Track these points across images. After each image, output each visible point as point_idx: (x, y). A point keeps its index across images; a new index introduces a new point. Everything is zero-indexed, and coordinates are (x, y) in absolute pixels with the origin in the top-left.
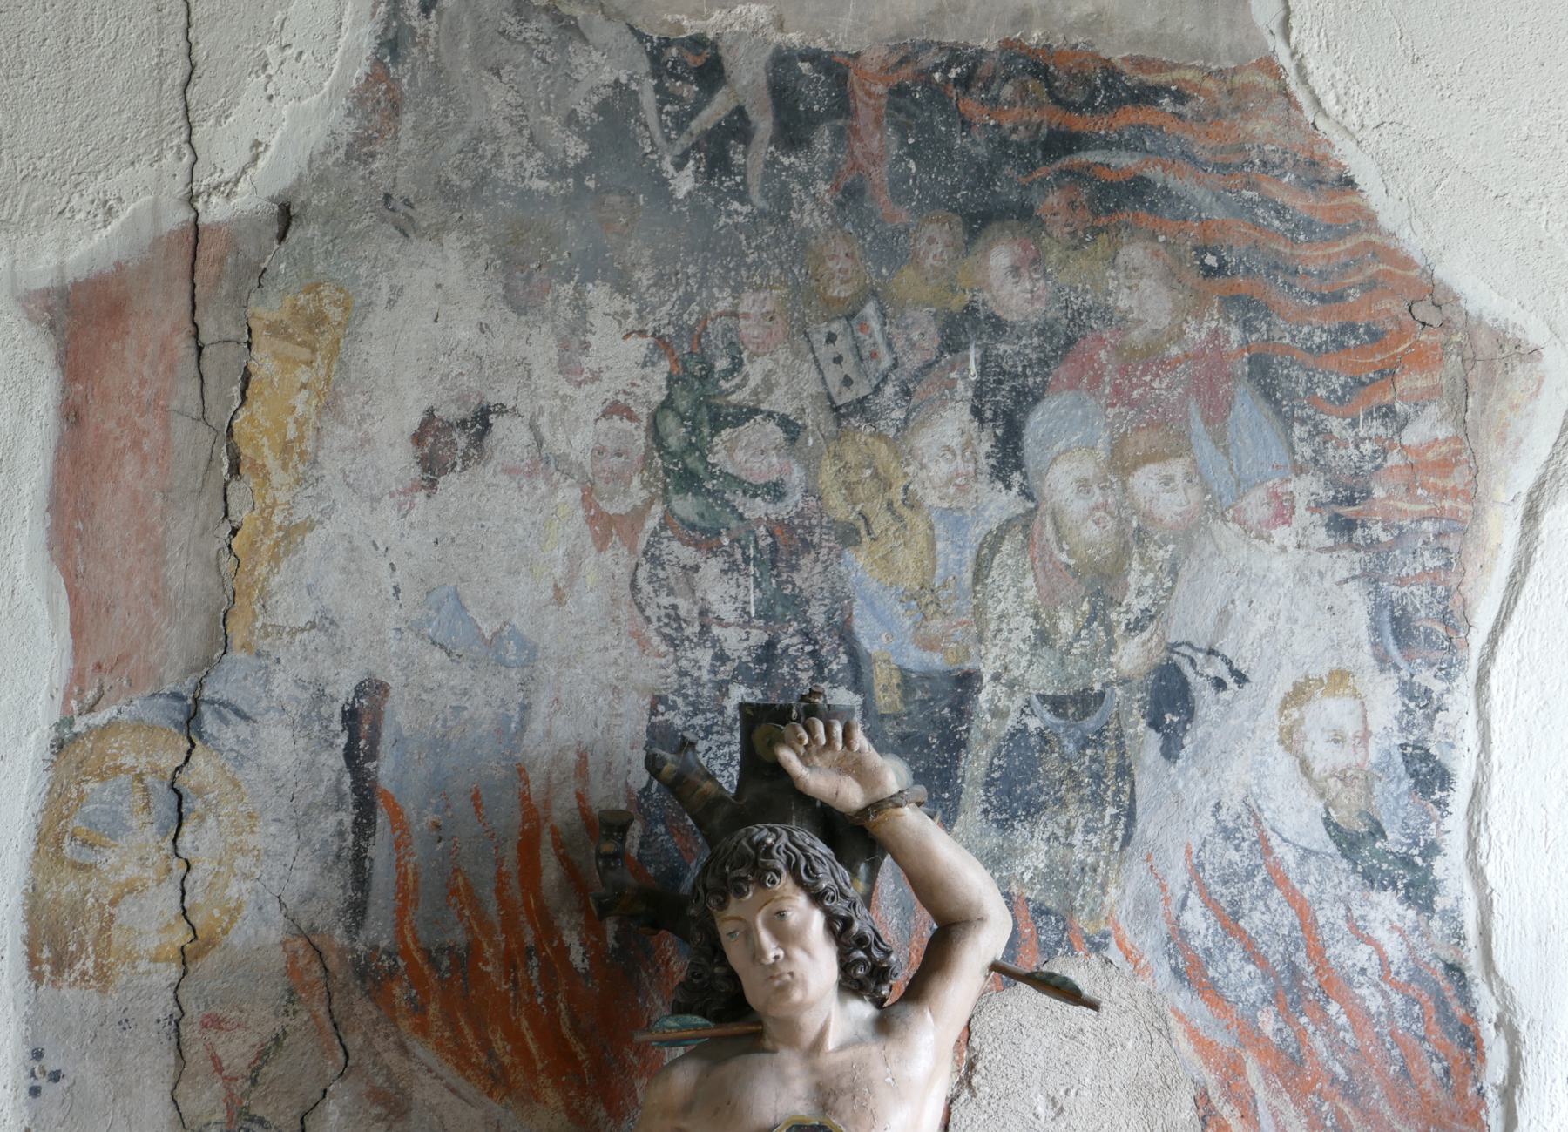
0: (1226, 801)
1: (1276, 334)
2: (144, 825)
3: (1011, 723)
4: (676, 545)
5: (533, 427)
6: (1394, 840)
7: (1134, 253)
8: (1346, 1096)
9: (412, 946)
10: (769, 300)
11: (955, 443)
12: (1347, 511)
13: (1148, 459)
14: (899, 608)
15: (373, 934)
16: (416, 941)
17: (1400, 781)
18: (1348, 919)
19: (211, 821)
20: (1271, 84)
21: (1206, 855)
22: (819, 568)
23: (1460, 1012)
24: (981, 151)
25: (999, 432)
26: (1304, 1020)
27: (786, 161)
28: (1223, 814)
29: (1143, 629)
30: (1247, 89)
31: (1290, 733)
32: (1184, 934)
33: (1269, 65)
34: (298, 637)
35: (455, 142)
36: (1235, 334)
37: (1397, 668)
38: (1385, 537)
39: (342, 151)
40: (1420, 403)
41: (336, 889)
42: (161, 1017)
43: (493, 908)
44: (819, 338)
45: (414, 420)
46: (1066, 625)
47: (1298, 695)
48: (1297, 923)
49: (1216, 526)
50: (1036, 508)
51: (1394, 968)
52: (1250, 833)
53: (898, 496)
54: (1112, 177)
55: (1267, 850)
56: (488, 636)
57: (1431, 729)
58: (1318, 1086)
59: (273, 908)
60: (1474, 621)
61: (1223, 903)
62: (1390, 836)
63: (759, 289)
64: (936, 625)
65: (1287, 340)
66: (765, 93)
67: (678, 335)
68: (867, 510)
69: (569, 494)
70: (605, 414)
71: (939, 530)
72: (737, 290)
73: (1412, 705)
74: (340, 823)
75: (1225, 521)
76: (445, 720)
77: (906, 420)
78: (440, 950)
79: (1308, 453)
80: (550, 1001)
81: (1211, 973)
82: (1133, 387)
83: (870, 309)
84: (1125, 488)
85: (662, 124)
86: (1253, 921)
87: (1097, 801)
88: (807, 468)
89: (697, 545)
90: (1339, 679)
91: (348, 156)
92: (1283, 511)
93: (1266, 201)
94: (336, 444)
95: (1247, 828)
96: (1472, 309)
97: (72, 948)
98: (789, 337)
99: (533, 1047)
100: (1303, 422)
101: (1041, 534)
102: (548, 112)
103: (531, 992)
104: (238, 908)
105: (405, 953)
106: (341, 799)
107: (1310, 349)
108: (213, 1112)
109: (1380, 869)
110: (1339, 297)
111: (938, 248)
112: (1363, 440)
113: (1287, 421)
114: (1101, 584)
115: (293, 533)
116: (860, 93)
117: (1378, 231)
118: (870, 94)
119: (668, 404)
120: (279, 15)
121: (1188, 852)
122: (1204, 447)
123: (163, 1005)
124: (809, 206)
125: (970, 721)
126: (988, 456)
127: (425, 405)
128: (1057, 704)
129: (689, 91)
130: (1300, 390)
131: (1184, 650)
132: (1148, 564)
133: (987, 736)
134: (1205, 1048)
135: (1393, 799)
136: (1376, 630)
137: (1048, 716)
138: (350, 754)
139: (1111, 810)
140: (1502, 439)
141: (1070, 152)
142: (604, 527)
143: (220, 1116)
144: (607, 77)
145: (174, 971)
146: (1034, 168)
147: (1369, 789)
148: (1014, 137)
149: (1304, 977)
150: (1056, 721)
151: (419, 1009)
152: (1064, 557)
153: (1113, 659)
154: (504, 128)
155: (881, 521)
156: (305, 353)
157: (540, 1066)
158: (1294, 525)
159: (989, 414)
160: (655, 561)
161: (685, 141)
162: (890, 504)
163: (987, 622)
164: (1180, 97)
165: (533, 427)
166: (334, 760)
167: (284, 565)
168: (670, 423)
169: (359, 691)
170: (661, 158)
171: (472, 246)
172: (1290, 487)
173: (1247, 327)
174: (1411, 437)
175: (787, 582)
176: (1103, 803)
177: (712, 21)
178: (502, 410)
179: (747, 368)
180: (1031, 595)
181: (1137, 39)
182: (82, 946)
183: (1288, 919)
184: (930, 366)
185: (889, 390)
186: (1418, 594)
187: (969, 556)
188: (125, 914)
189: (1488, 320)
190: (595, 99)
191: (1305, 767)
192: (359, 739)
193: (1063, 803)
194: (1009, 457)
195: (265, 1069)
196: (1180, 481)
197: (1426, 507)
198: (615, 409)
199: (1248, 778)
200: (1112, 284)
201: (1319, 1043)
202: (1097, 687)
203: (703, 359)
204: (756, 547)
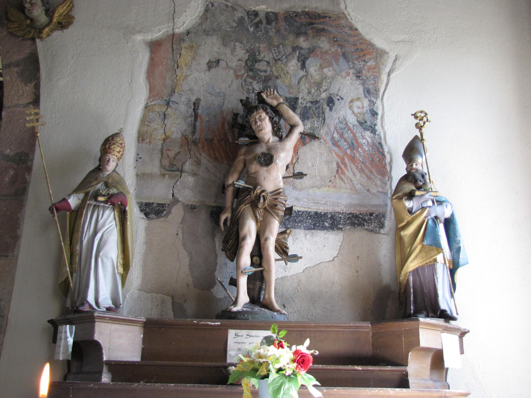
3: (304, 105)
5: (226, 62)
6: (369, 123)
7: (323, 39)
10: (265, 45)
13: (325, 67)
18: (362, 135)
30: (340, 17)
32: (334, 138)
33: (343, 14)
35: (215, 24)
36: (339, 50)
40: (370, 60)
41: (190, 130)
44: (273, 50)
45: (207, 61)
46: (313, 91)
47: (352, 101)
49: (337, 77)
52: (344, 122)
53: (285, 72)
55: (347, 125)
59: (179, 132)
69: (232, 72)
72: (260, 44)
83: (281, 46)
86: (346, 136)
87: (319, 117)
90: (358, 99)
92: (348, 74)
95: (344, 121)
110: (356, 45)
113: (348, 62)
114: (319, 85)
115: (186, 76)
119: (248, 59)
123: (160, 147)
128: (312, 102)
129: (253, 17)
132: (326, 82)
134: (338, 156)
138: (194, 109)
140: (383, 65)
142: (237, 77)
144: (240, 15)
145: (162, 142)
155: (282, 75)
161: (252, 24)
164: (330, 17)
165: (226, 62)
166: (191, 110)
169: (196, 100)
173: (341, 49)
174: (368, 64)
178: (221, 60)
180: (307, 86)
182: (147, 138)
184: (290, 54)
185: (284, 57)
186: (371, 87)
187: (297, 81)
191: (353, 112)
193: (313, 117)
194: (303, 66)
198: (239, 60)
199: (344, 114)
201: (357, 155)
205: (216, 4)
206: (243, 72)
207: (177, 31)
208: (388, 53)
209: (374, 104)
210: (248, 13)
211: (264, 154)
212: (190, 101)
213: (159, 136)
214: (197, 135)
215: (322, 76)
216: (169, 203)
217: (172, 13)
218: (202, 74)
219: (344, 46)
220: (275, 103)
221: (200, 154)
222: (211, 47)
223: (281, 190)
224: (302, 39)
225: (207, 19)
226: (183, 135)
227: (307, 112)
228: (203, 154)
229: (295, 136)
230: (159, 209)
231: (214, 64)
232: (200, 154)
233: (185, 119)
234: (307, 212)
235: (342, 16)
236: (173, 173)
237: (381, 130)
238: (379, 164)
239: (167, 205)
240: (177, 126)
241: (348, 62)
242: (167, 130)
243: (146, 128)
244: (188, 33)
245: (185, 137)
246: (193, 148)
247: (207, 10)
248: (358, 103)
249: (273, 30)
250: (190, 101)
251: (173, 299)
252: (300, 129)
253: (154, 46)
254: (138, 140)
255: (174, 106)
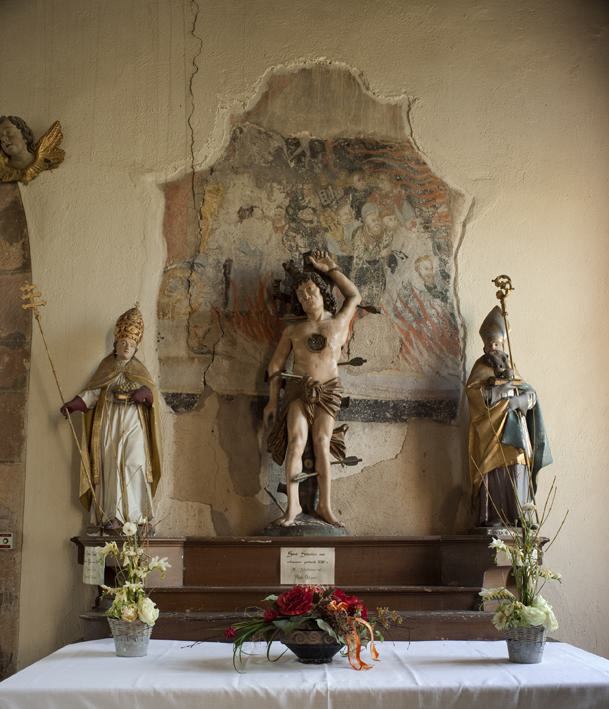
6: (439, 288)
7: (382, 176)
10: (310, 186)
33: (408, 142)
35: (246, 157)
41: (221, 301)
45: (238, 209)
46: (371, 247)
47: (418, 260)
55: (413, 291)
69: (269, 223)
83: (330, 187)
86: (411, 305)
90: (427, 257)
95: (409, 286)
114: (378, 239)
119: (289, 206)
122: (398, 213)
128: (369, 262)
134: (402, 330)
135: (438, 280)
138: (225, 274)
142: (276, 229)
151: (239, 324)
164: (391, 147)
166: (221, 275)
184: (341, 198)
186: (442, 241)
191: (420, 275)
194: (358, 215)
198: (279, 207)
205: (245, 130)
206: (284, 223)
207: (198, 169)
208: (463, 196)
209: (446, 263)
210: (287, 141)
211: (314, 335)
212: (219, 262)
213: (183, 308)
214: (230, 308)
217: (191, 142)
218: (233, 226)
219: (409, 187)
220: (326, 268)
221: (235, 331)
222: (241, 191)
223: (336, 380)
224: (356, 178)
225: (235, 151)
226: (213, 307)
227: (364, 275)
228: (240, 332)
229: (351, 310)
231: (245, 213)
232: (235, 331)
233: (214, 286)
235: (407, 145)
237: (454, 298)
240: (204, 295)
241: (415, 208)
242: (192, 302)
243: (166, 300)
244: (212, 170)
245: (215, 310)
246: (227, 324)
247: (234, 139)
248: (426, 263)
249: (320, 165)
251: (212, 507)
252: (356, 301)
253: (170, 189)
254: (158, 315)
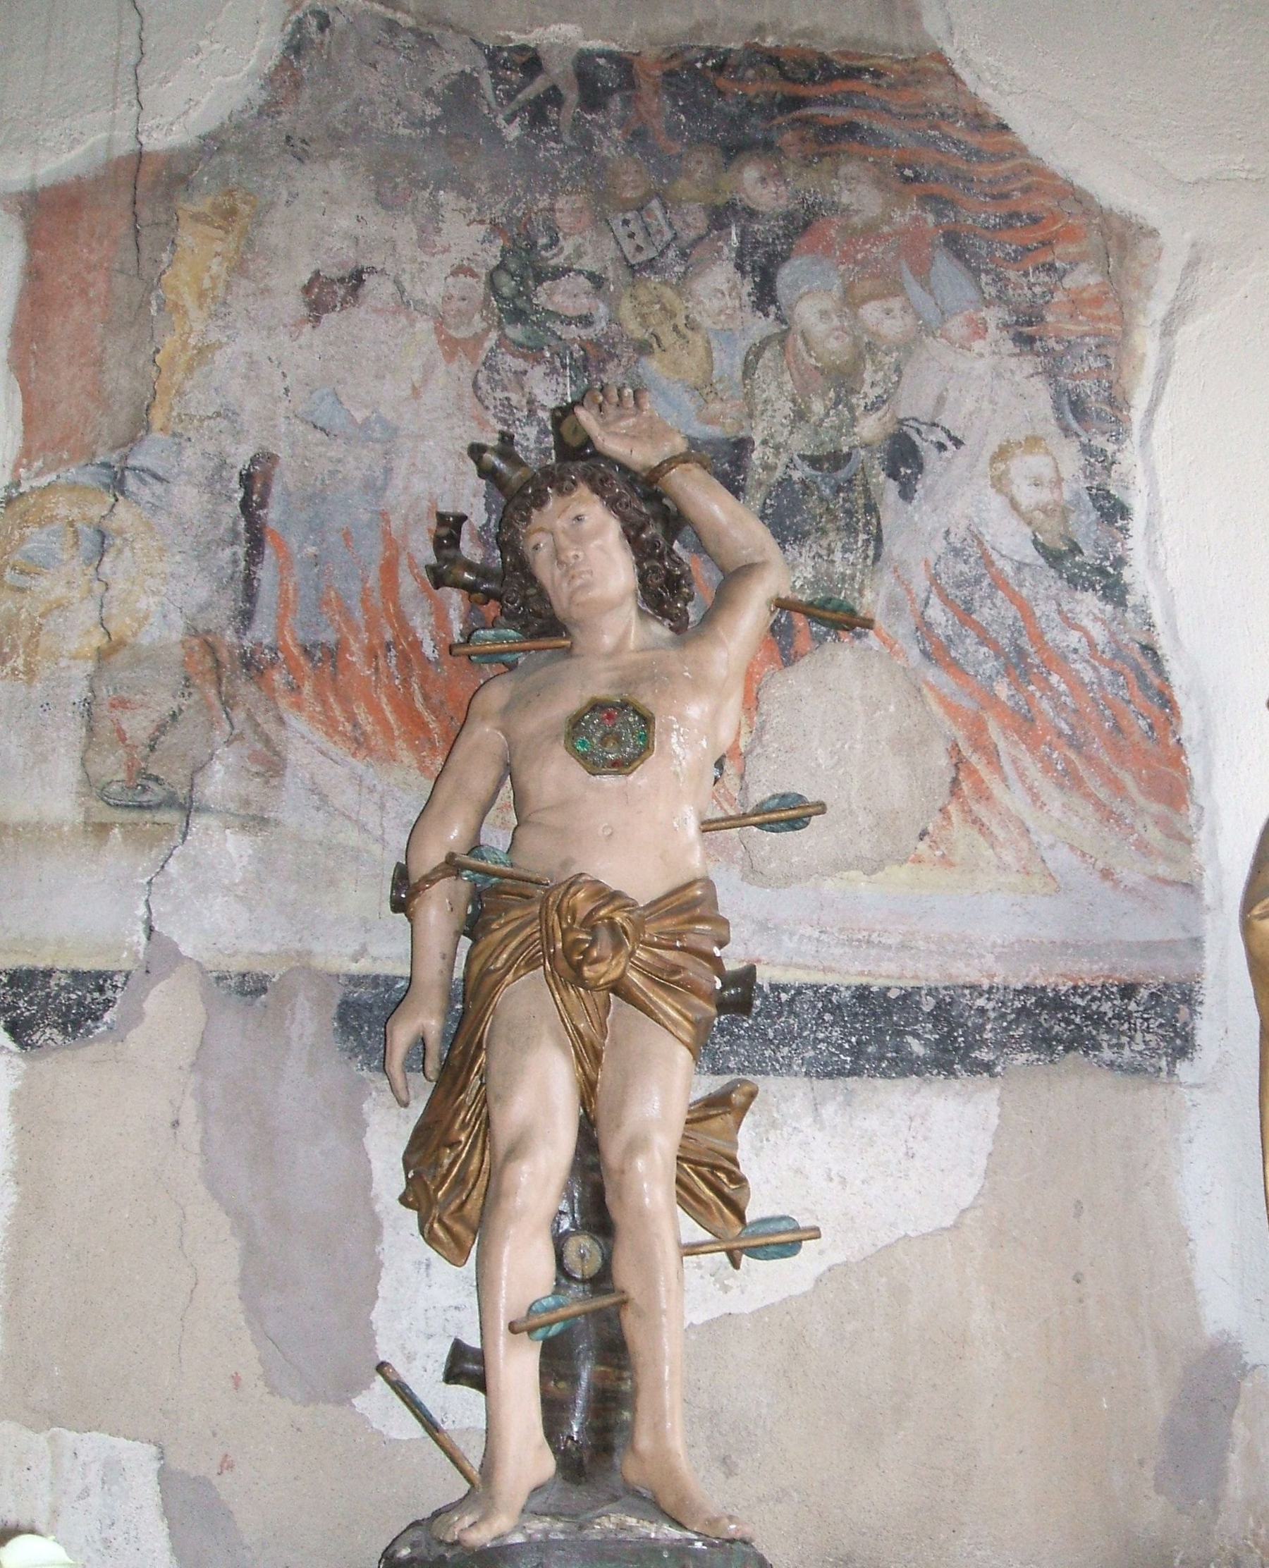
0: (953, 530)
1: (961, 219)
2: (73, 557)
3: (778, 474)
4: (509, 358)
5: (397, 282)
6: (1089, 555)
7: (849, 169)
8: (1071, 746)
9: (290, 642)
10: (579, 201)
11: (725, 287)
12: (1027, 330)
13: (872, 297)
14: (686, 397)
15: (258, 634)
16: (295, 639)
17: (1089, 513)
18: (1060, 612)
19: (127, 553)
20: (941, 68)
21: (941, 567)
22: (621, 370)
23: (1157, 682)
24: (735, 110)
25: (757, 279)
26: (1031, 688)
27: (589, 117)
28: (952, 538)
29: (878, 409)
30: (926, 71)
31: (999, 479)
32: (929, 625)
33: (939, 57)
34: (206, 423)
35: (341, 107)
36: (931, 218)
37: (1078, 436)
38: (1059, 348)
39: (255, 110)
40: (1074, 263)
41: (227, 603)
42: (77, 700)
43: (358, 615)
44: (617, 223)
45: (305, 278)
46: (818, 407)
47: (1002, 454)
48: (1019, 616)
49: (929, 341)
50: (790, 328)
51: (1099, 648)
52: (975, 551)
53: (681, 322)
54: (832, 123)
55: (990, 564)
56: (359, 420)
57: (1109, 476)
58: (1048, 738)
59: (175, 617)
60: (1133, 403)
61: (958, 601)
62: (1086, 553)
63: (570, 193)
64: (716, 407)
65: (970, 222)
66: (572, 77)
67: (509, 223)
68: (659, 331)
69: (424, 326)
70: (454, 274)
71: (714, 344)
72: (554, 195)
73: (1092, 460)
74: (235, 554)
75: (935, 337)
76: (323, 481)
77: (685, 273)
78: (314, 645)
79: (994, 293)
80: (406, 682)
81: (953, 654)
82: (857, 252)
83: (655, 204)
84: (856, 316)
85: (496, 97)
86: (984, 614)
87: (851, 530)
88: (609, 305)
89: (525, 357)
90: (1033, 443)
91: (260, 113)
92: (979, 330)
93: (945, 137)
94: (241, 292)
95: (972, 547)
96: (1105, 204)
97: (7, 650)
98: (594, 222)
99: (391, 718)
100: (987, 272)
101: (795, 346)
102: (412, 88)
103: (391, 677)
104: (146, 618)
105: (285, 649)
106: (236, 535)
107: (987, 228)
108: (116, 772)
109: (1081, 576)
110: (1005, 196)
111: (705, 167)
112: (1034, 284)
113: (976, 272)
114: (843, 380)
115: (204, 352)
116: (642, 75)
117: (1029, 157)
118: (649, 76)
119: (502, 266)
120: (211, 24)
121: (926, 563)
122: (914, 290)
123: (79, 691)
124: (606, 143)
125: (745, 473)
126: (749, 295)
127: (314, 268)
128: (814, 462)
129: (516, 77)
130: (984, 252)
131: (911, 423)
132: (879, 367)
133: (760, 484)
134: (953, 710)
135: (1085, 525)
136: (1058, 409)
137: (807, 469)
138: (245, 504)
139: (862, 537)
140: (1138, 284)
141: (799, 108)
142: (451, 347)
143: (122, 775)
144: (456, 68)
145: (90, 666)
146: (773, 118)
147: (1065, 519)
148: (758, 101)
149: (1029, 655)
150: (814, 472)
151: (295, 689)
152: (813, 361)
153: (856, 430)
154: (379, 98)
155: (669, 338)
156: (221, 233)
157: (396, 733)
158: (988, 340)
159: (748, 268)
160: (492, 368)
161: (514, 106)
162: (675, 328)
163: (756, 405)
164: (877, 74)
165: (397, 282)
166: (232, 510)
167: (196, 374)
168: (503, 279)
169: (253, 461)
170: (495, 117)
171: (353, 168)
172: (983, 314)
173: (939, 214)
174: (1068, 282)
175: (596, 380)
176: (856, 532)
177: (532, 36)
178: (372, 271)
179: (562, 243)
180: (789, 387)
181: (843, 40)
182: (14, 647)
183: (1011, 612)
184: (701, 238)
185: (671, 253)
186: (1088, 386)
187: (739, 361)
188: (52, 623)
189: (1116, 211)
190: (447, 82)
191: (1014, 505)
192: (253, 494)
193: (824, 532)
194: (765, 296)
195: (163, 738)
196: (897, 312)
197: (1086, 328)
198: (459, 270)
199: (971, 511)
200: (836, 189)
201: (1045, 705)
202: (845, 449)
203: (528, 237)
204: (571, 358)
205: (339, 21)
206: (478, 324)
207: (156, 142)
209: (1109, 464)
210: (493, 58)
212: (223, 465)
214: (263, 631)
215: (856, 342)
216: (126, 966)
217: (133, 59)
219: (951, 203)
222: (325, 215)
224: (751, 174)
225: (298, 85)
226: (192, 631)
227: (795, 507)
228: (298, 723)
230: (80, 1003)
232: (281, 721)
233: (203, 552)
234: (815, 988)
235: (931, 67)
236: (148, 816)
238: (1148, 745)
239: (119, 980)
246: (247, 691)
247: (296, 47)
248: (1037, 463)
250: (223, 465)
255: (146, 494)
